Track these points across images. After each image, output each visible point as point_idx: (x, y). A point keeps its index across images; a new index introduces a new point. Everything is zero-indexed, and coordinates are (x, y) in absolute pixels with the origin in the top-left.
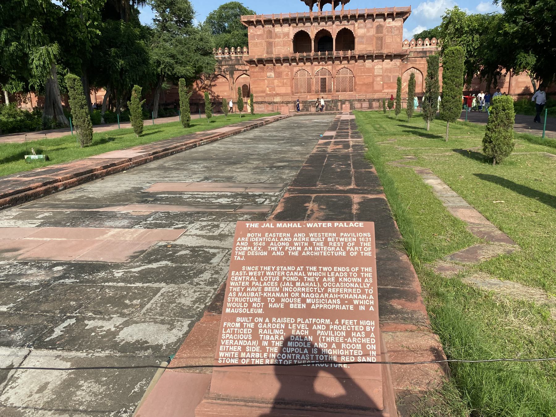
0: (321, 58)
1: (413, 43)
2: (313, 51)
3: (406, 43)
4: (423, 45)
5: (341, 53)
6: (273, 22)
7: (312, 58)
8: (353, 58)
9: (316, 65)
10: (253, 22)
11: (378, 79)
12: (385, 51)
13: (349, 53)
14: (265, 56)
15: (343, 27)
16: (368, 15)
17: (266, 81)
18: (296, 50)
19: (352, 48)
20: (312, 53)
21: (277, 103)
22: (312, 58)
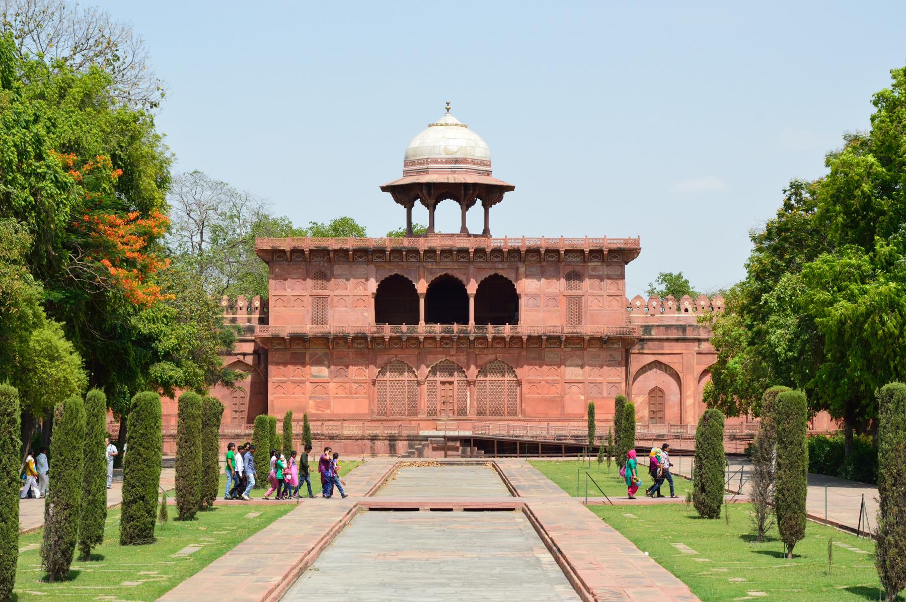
0: (442, 338)
1: (654, 303)
2: (422, 322)
3: (638, 303)
4: (679, 309)
5: (490, 330)
6: (332, 255)
7: (421, 338)
8: (516, 339)
9: (430, 353)
10: (283, 251)
11: (575, 389)
12: (588, 329)
13: (507, 330)
14: (309, 329)
15: (492, 273)
16: (548, 251)
17: (308, 384)
18: (381, 317)
19: (513, 319)
20: (422, 328)
21: (348, 438)
22: (421, 338)
